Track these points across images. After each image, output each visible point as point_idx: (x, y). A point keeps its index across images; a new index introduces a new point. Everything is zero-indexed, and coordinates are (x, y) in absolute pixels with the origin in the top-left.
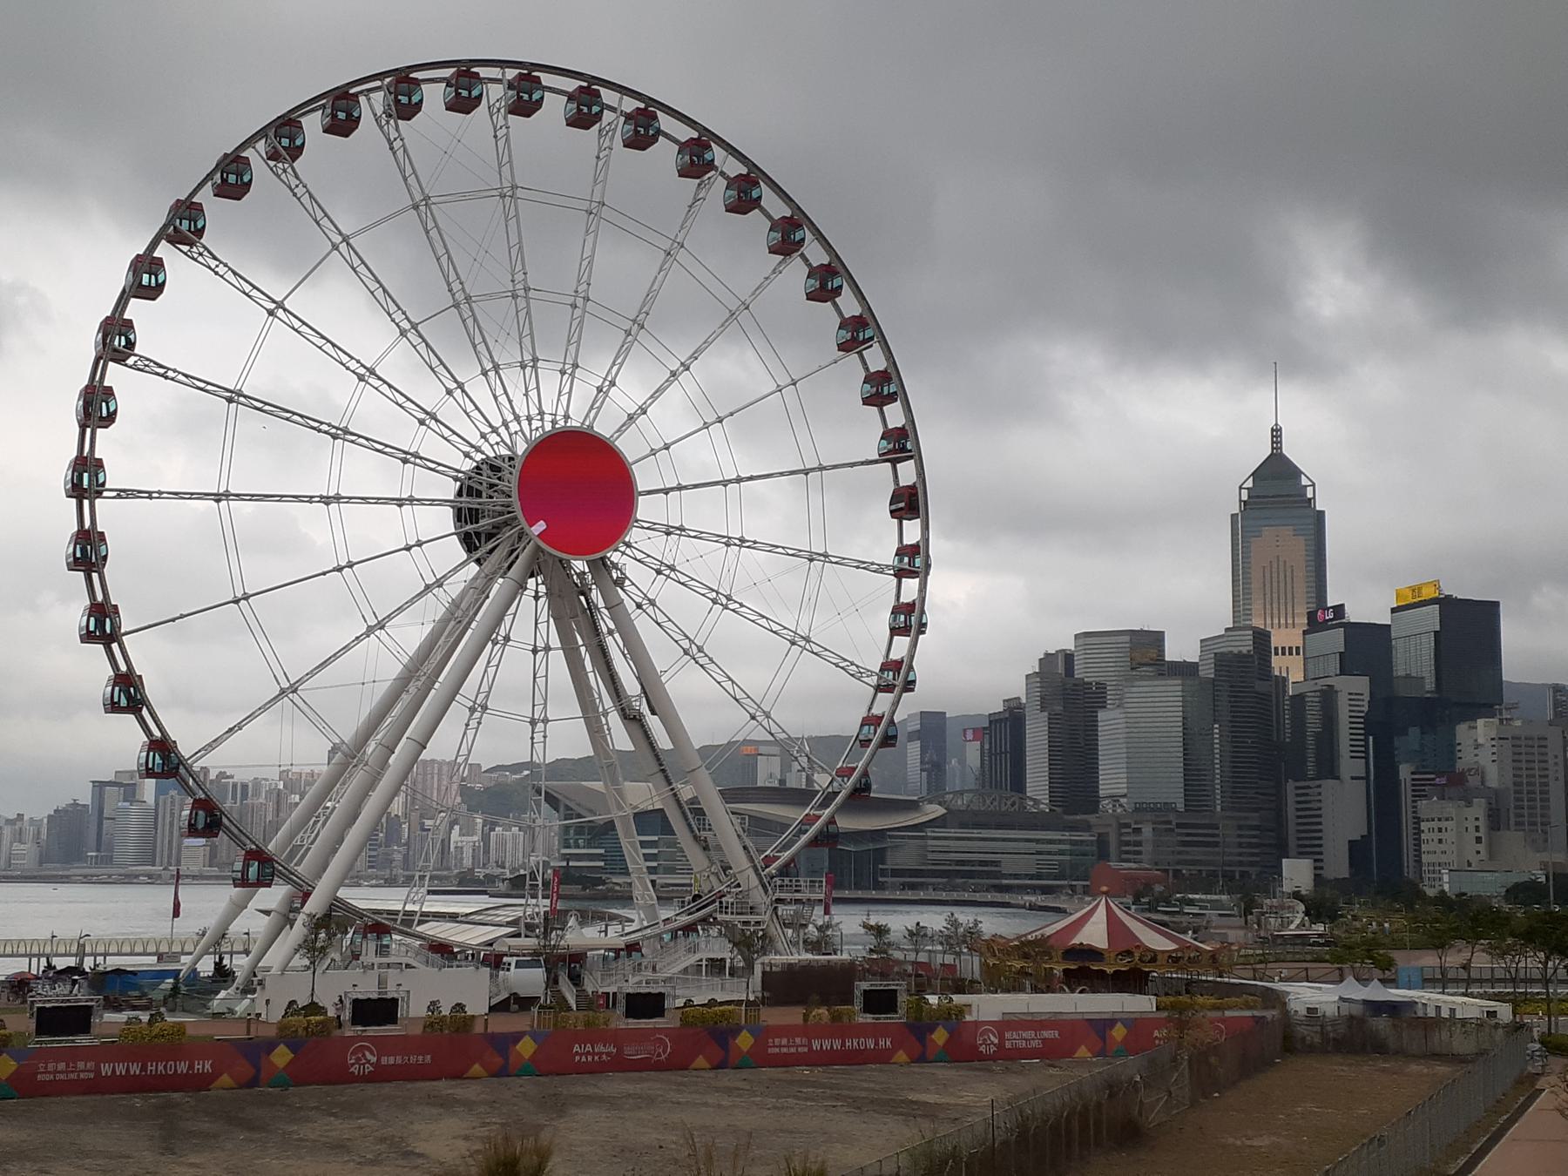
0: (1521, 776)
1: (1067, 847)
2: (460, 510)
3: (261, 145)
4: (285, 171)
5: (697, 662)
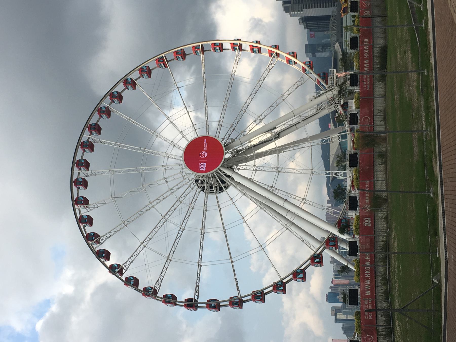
2: (210, 193)
3: (95, 246)
4: (102, 240)
5: (264, 118)
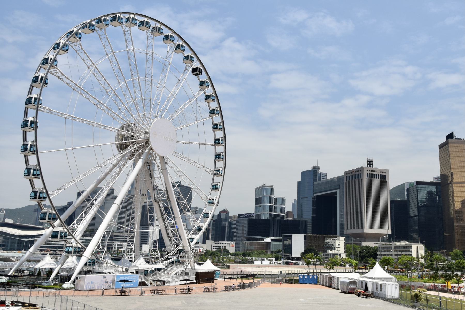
1: (84, 241)
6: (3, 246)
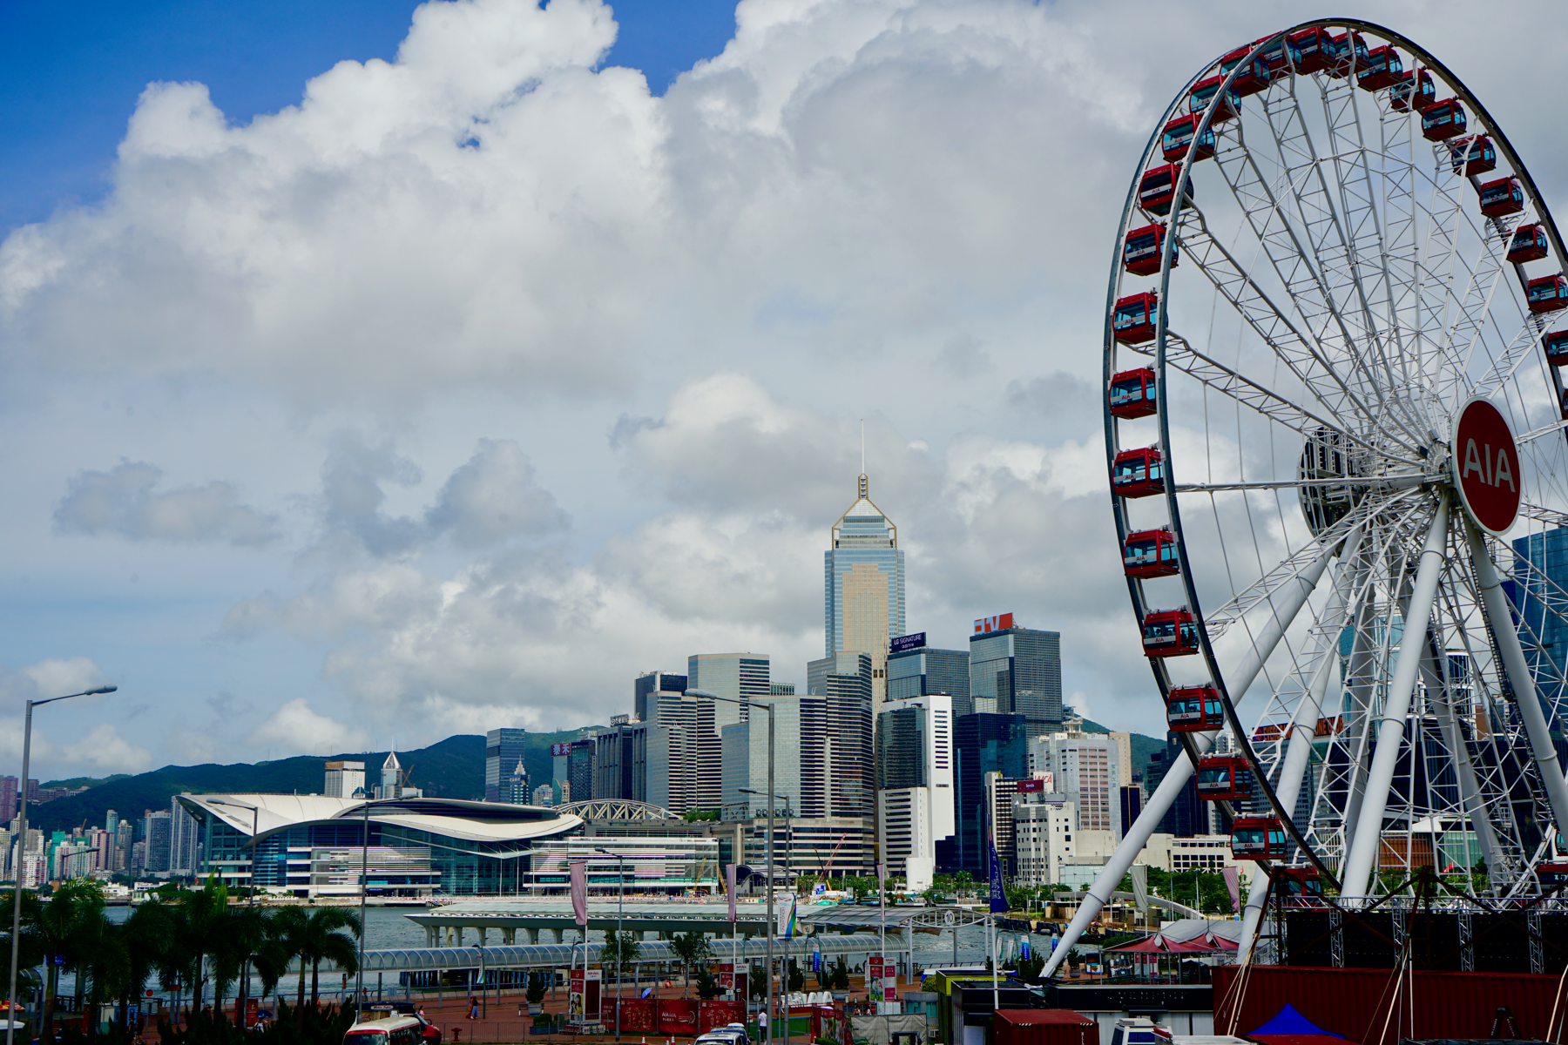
0: (1086, 783)
1: (693, 852)
6: (436, 879)
